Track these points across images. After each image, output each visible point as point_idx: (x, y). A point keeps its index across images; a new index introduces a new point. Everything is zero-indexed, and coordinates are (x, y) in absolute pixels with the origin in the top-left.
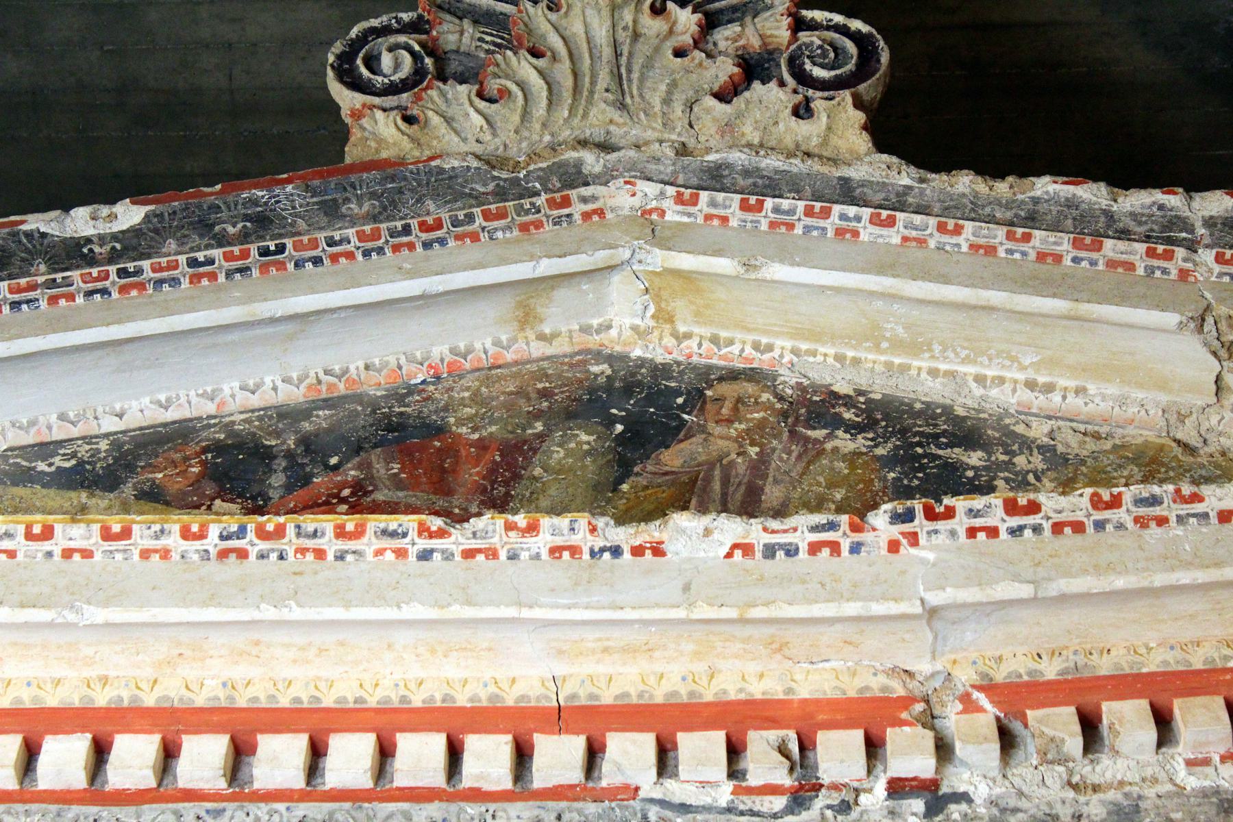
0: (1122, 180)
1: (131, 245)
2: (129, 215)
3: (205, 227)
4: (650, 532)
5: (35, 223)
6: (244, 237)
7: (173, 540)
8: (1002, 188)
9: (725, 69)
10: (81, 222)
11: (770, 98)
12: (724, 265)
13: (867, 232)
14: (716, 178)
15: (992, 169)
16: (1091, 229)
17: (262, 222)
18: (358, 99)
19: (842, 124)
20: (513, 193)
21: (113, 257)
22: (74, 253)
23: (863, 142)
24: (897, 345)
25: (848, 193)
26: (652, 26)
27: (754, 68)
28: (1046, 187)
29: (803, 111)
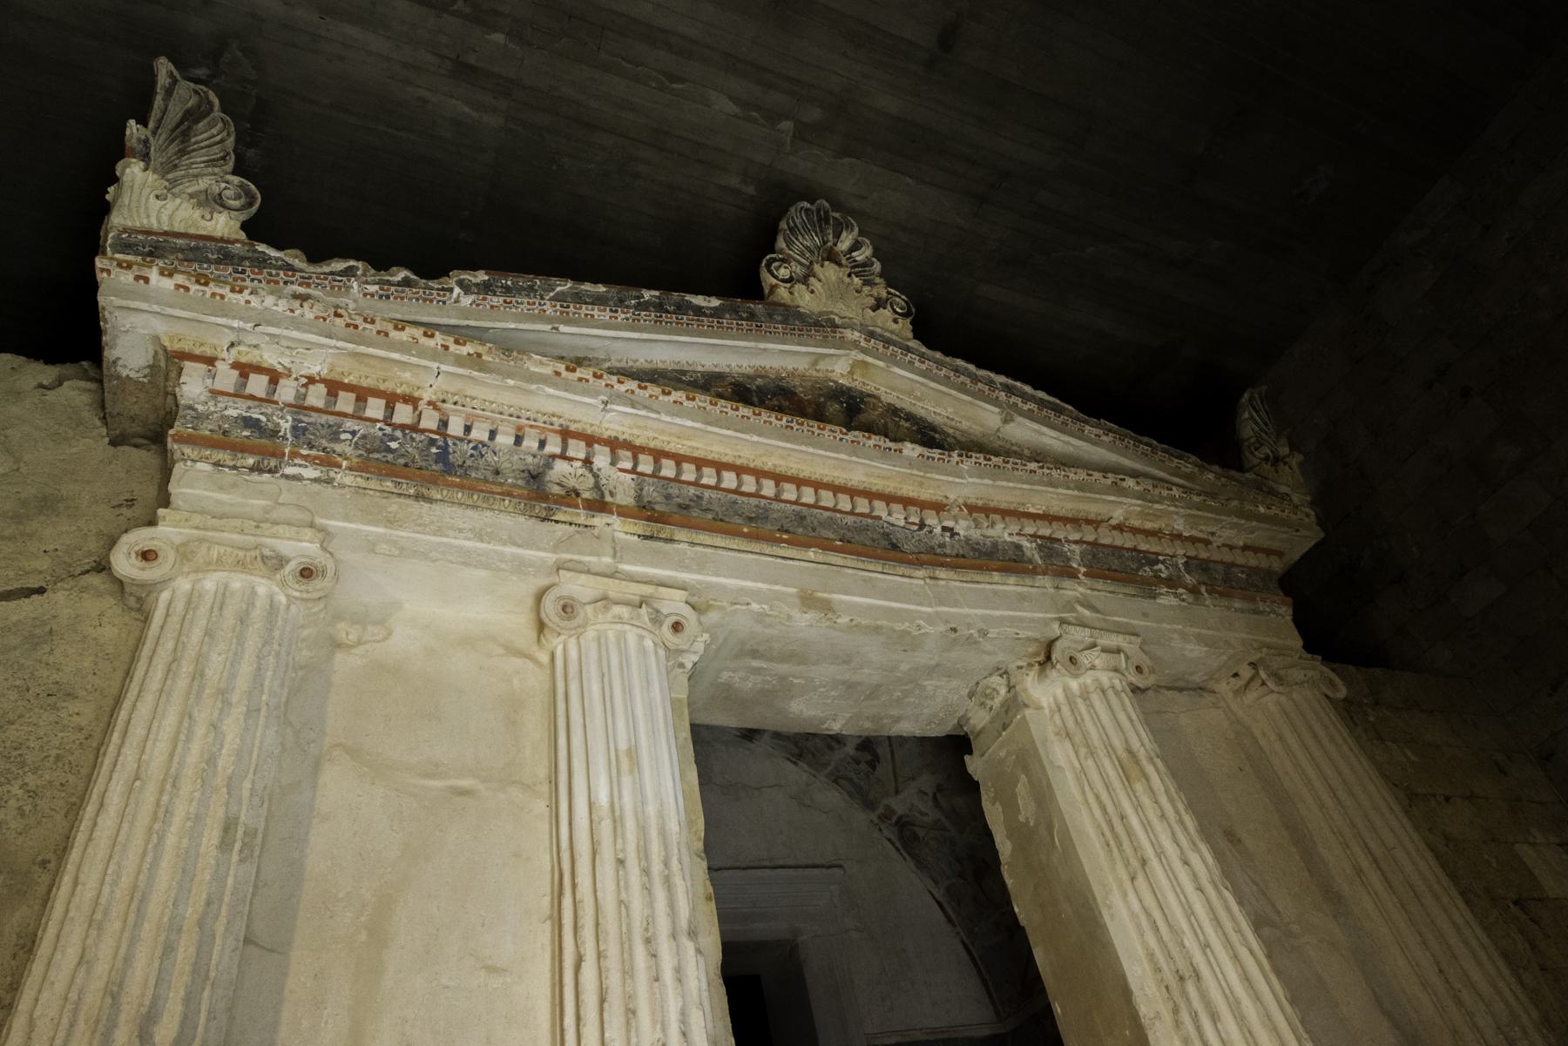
0: (979, 366)
1: (716, 313)
2: (715, 302)
3: (735, 311)
4: (899, 445)
5: (688, 297)
6: (747, 319)
7: (773, 419)
8: (948, 359)
9: (872, 301)
10: (699, 300)
11: (886, 314)
12: (881, 364)
13: (917, 364)
14: (871, 335)
15: (946, 354)
16: (976, 379)
17: (752, 316)
18: (774, 281)
19: (904, 328)
20: (821, 327)
21: (712, 316)
22: (699, 311)
23: (910, 335)
24: (916, 398)
25: (908, 350)
26: (847, 280)
27: (879, 304)
28: (960, 362)
29: (895, 321)
